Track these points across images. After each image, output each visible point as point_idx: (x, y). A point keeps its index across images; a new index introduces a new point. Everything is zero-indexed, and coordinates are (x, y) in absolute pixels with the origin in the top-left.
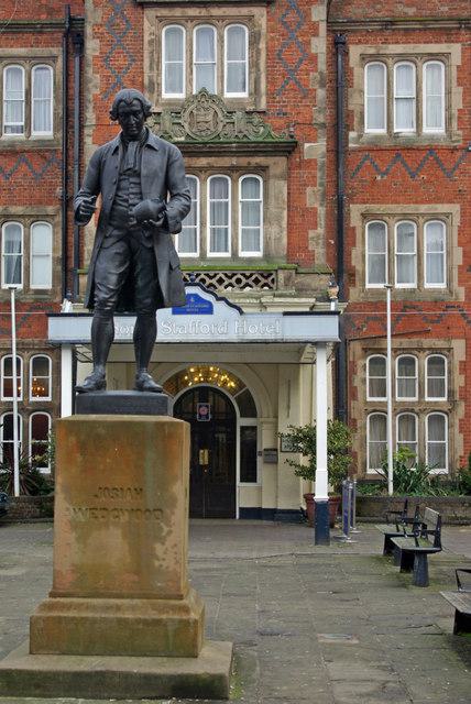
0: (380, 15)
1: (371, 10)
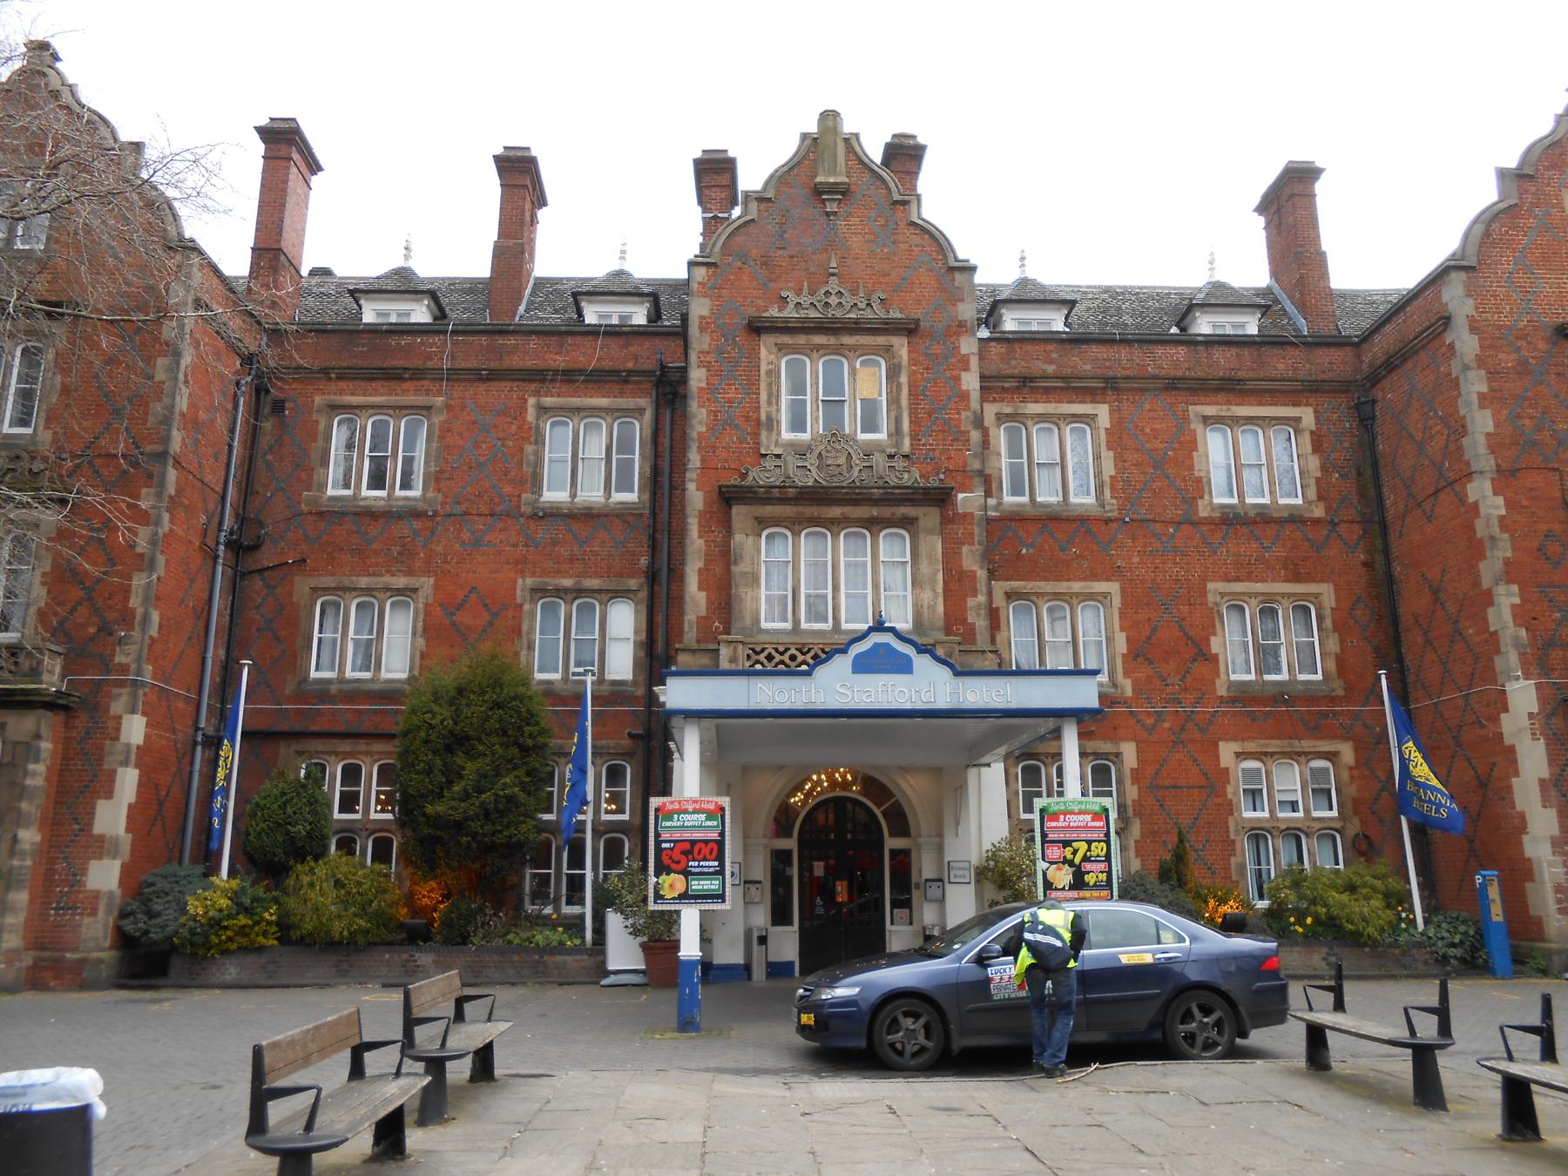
0: (1016, 371)
1: (1006, 366)
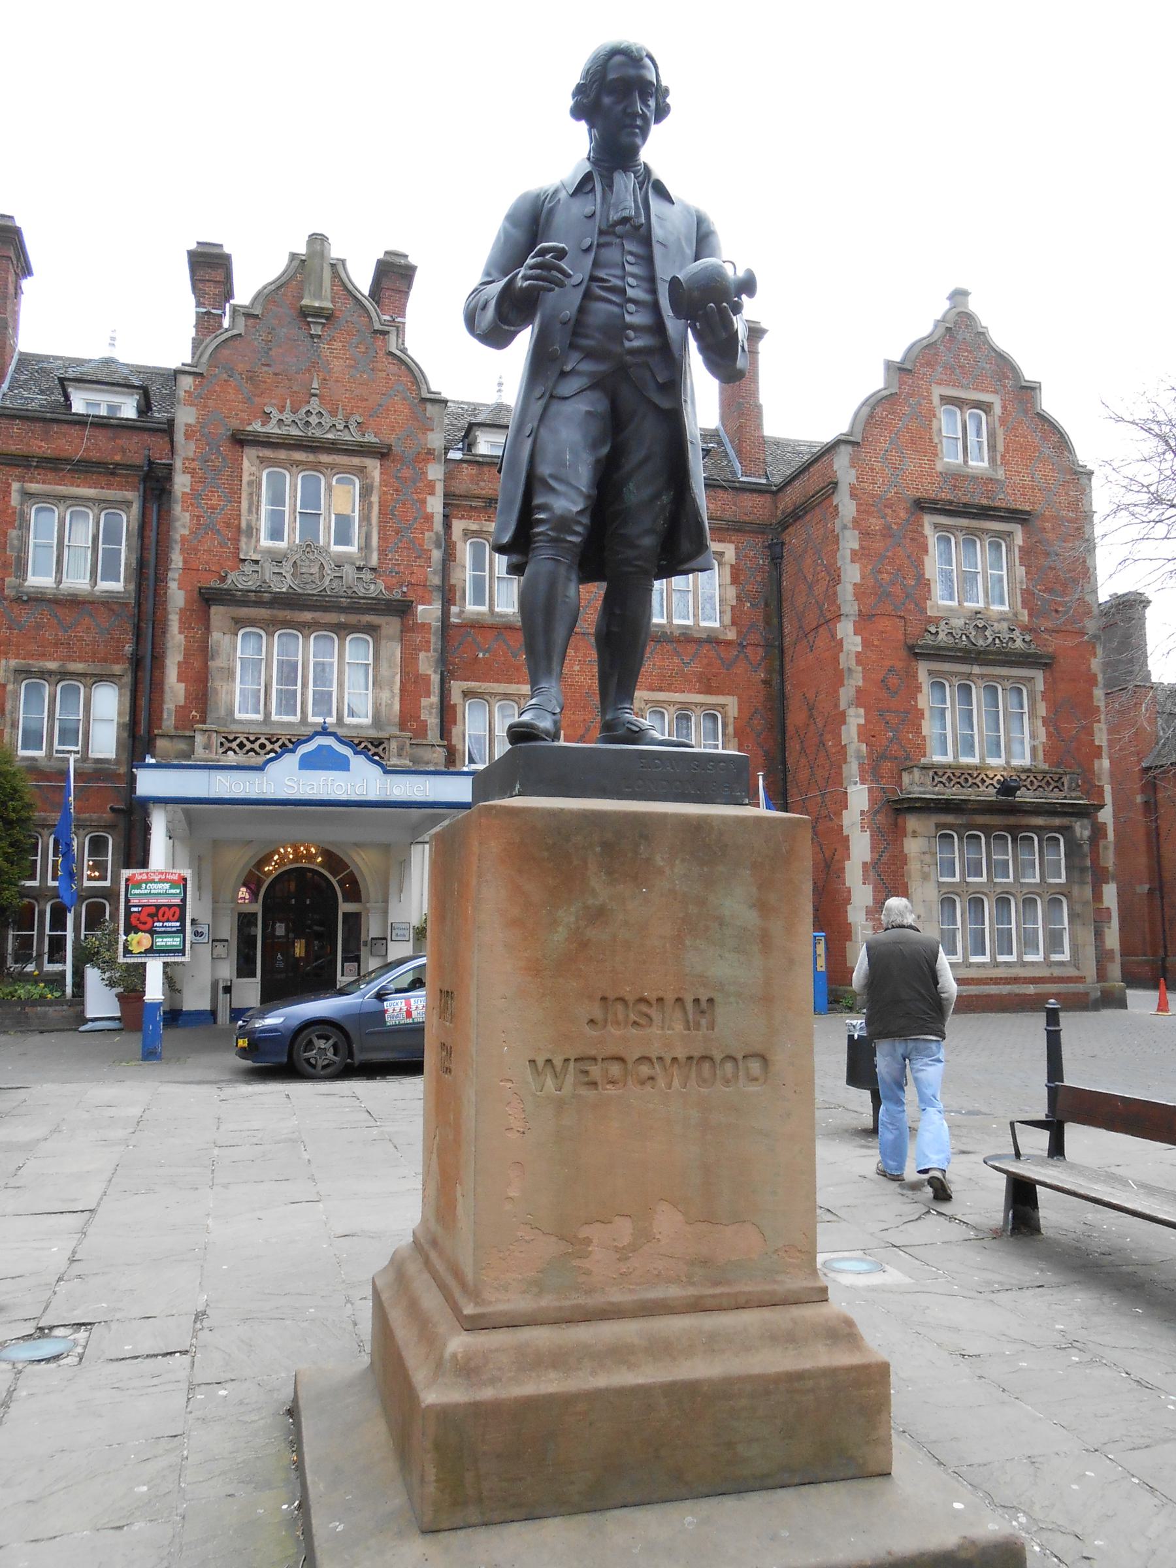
0: (484, 492)
1: (475, 487)
